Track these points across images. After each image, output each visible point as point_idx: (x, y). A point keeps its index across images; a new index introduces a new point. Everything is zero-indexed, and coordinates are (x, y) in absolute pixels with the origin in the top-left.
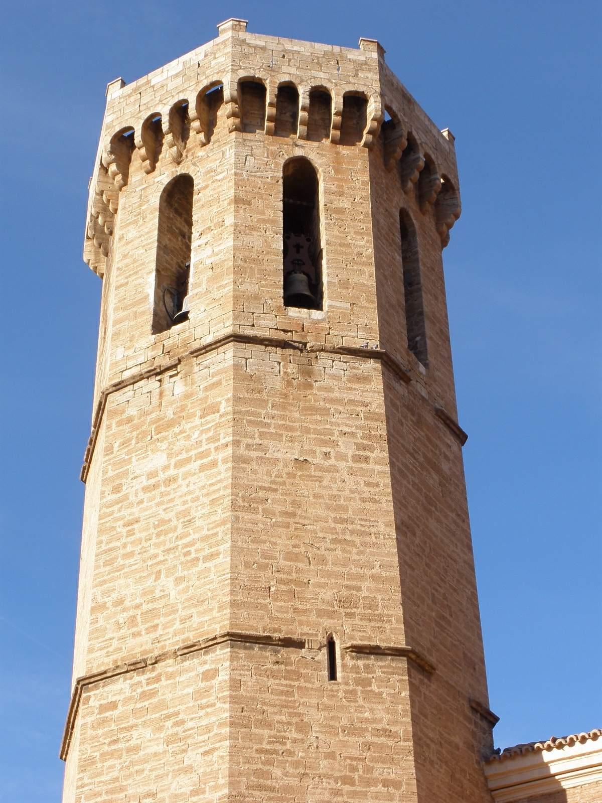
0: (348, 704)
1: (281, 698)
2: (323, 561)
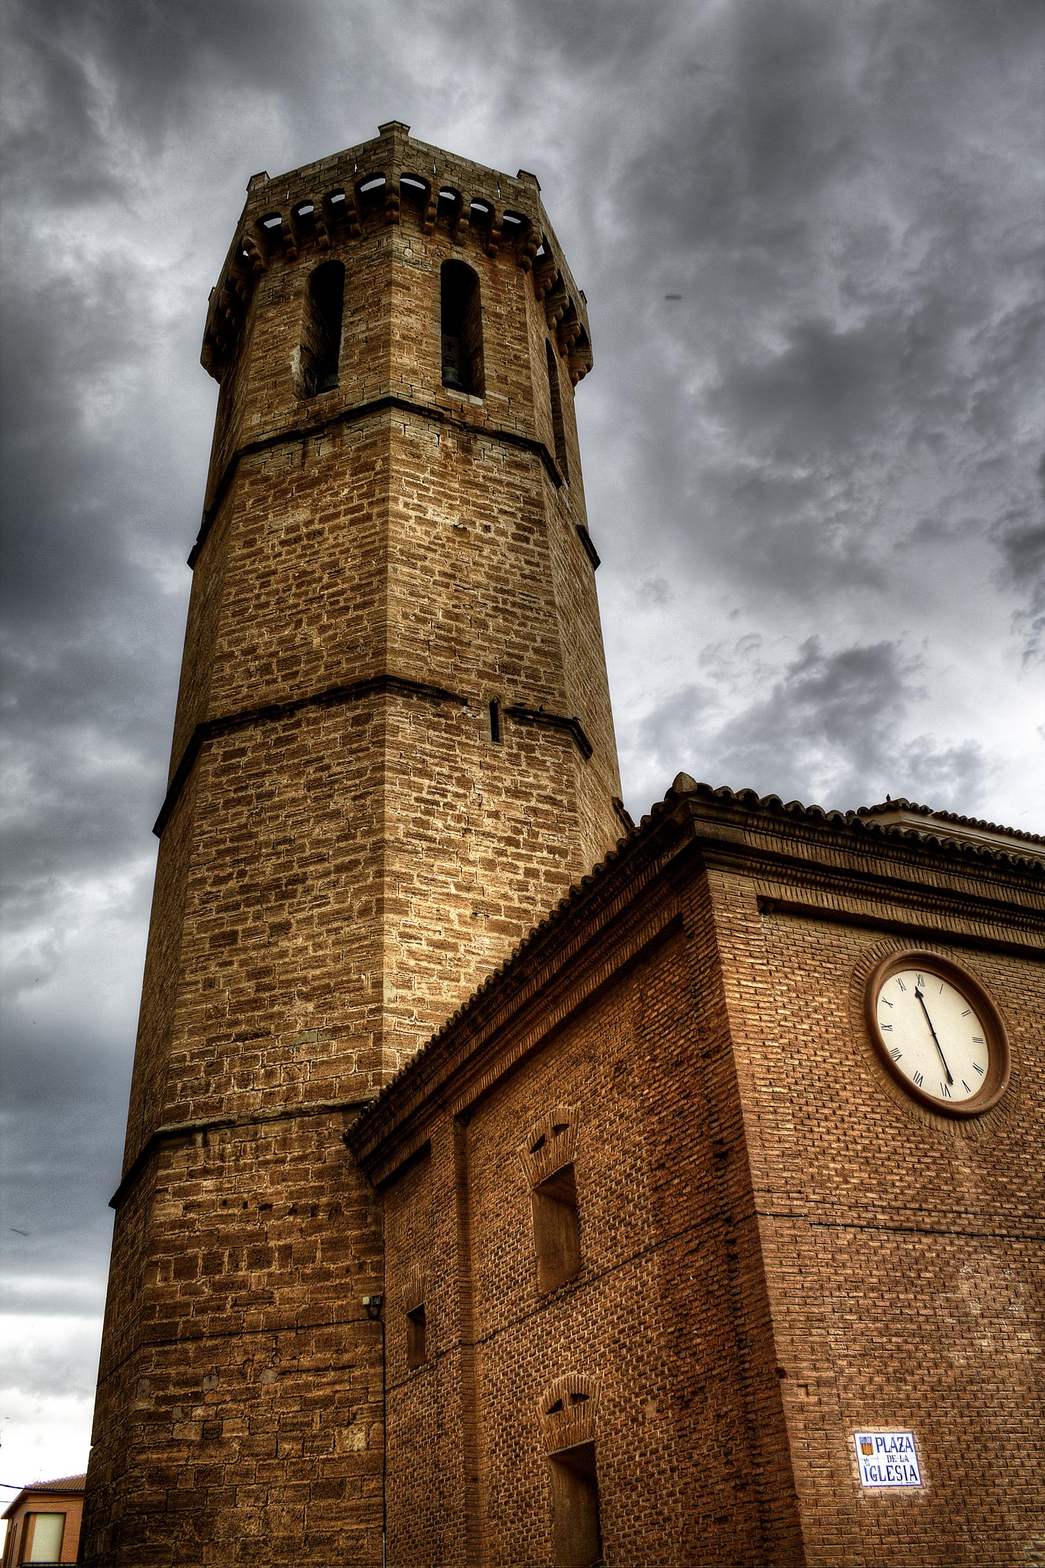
2: (485, 626)
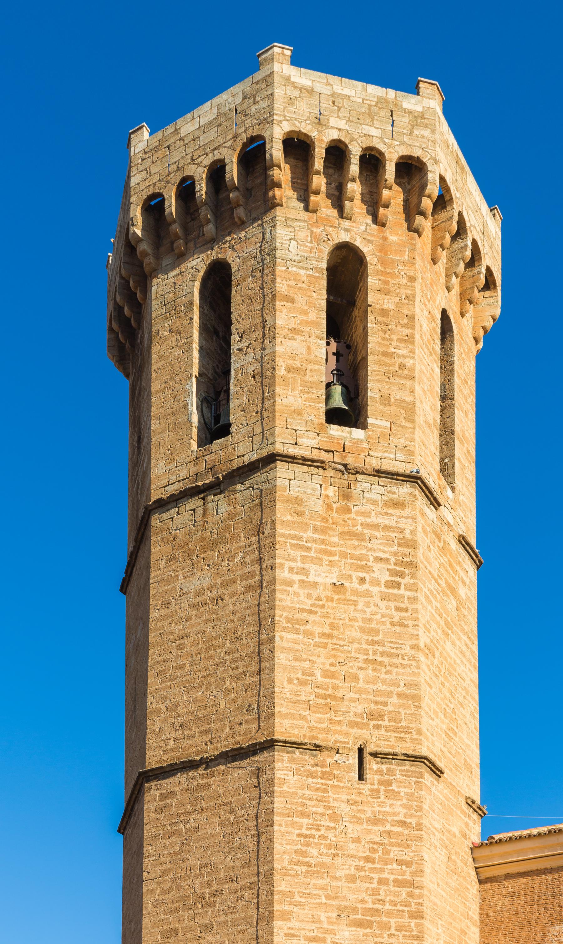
0: (372, 800)
1: (317, 793)
2: (356, 679)
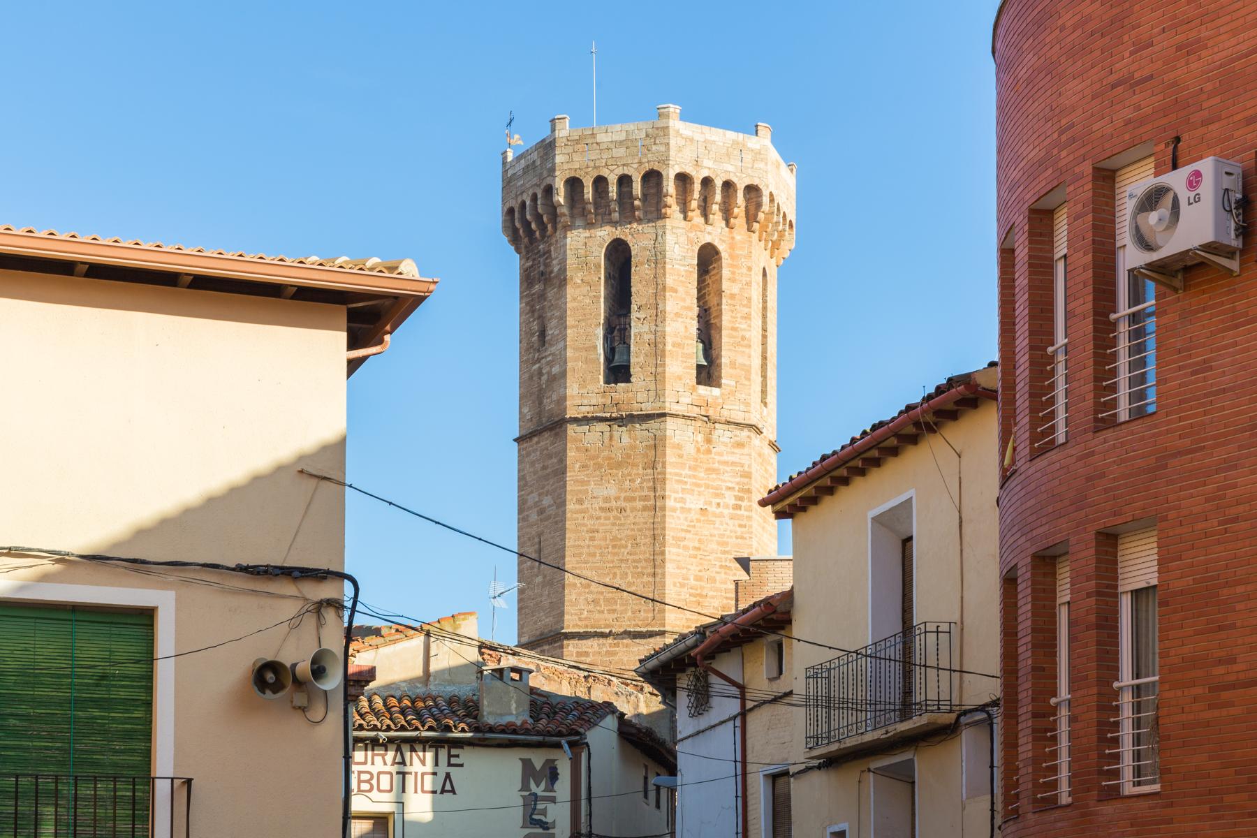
2: (714, 581)
